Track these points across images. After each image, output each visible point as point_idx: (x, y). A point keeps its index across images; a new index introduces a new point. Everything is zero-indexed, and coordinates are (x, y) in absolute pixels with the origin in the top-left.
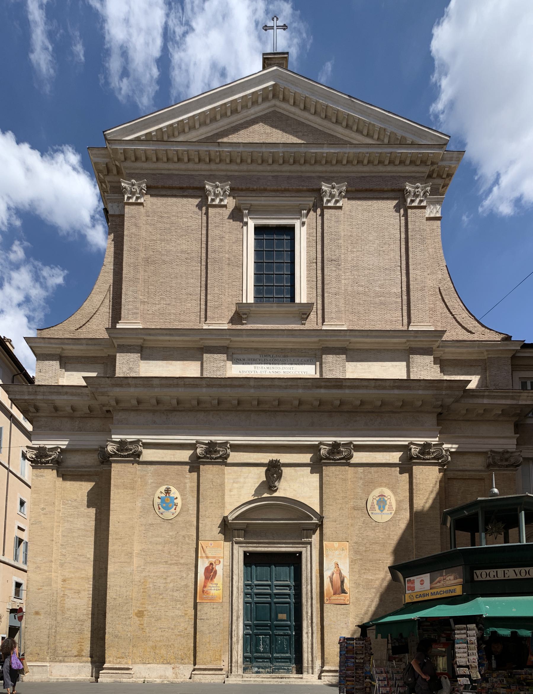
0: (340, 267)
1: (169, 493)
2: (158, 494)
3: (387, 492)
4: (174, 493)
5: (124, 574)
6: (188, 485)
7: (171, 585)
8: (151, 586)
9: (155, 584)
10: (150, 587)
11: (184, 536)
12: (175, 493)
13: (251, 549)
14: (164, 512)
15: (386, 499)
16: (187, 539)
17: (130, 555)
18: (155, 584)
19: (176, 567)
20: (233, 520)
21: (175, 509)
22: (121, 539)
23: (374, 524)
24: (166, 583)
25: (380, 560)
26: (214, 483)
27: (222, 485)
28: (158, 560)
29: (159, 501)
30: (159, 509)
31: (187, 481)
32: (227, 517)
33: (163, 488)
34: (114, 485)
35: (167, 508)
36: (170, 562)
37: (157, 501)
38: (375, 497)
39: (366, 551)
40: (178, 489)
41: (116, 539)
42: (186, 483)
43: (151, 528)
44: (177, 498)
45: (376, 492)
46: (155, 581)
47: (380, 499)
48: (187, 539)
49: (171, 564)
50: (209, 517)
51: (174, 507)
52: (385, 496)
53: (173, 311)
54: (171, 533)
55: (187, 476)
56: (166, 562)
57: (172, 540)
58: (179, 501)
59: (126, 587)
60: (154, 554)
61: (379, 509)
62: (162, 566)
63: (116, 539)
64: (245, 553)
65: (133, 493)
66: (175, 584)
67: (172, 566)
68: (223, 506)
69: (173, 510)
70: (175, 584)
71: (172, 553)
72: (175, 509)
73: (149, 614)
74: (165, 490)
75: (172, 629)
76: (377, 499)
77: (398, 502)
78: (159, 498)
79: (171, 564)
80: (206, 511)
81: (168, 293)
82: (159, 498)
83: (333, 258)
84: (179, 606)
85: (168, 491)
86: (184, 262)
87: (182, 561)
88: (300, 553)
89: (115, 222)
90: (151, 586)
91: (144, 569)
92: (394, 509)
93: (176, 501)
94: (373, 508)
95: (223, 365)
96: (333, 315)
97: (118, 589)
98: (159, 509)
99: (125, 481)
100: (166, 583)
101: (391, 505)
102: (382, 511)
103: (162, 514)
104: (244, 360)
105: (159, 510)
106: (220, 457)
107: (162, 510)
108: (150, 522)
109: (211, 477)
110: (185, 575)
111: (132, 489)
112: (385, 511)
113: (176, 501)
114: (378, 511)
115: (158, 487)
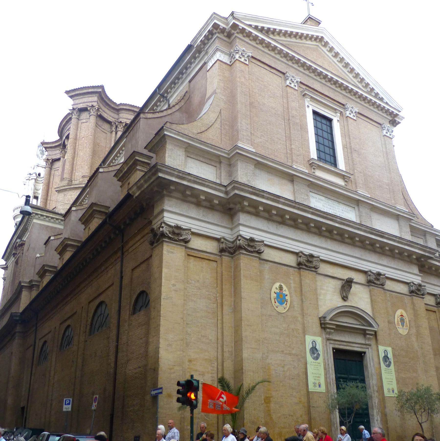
0: (360, 156)
1: (282, 290)
2: (274, 290)
3: (404, 314)
4: (285, 290)
6: (292, 285)
7: (288, 374)
8: (274, 373)
11: (293, 329)
12: (286, 291)
13: (337, 346)
14: (278, 306)
16: (295, 332)
18: (276, 371)
20: (330, 320)
21: (286, 305)
23: (400, 335)
24: (284, 371)
25: (406, 363)
27: (316, 290)
29: (275, 295)
30: (275, 302)
31: (292, 282)
32: (325, 318)
33: (277, 285)
35: (281, 303)
36: (285, 352)
37: (273, 295)
38: (398, 316)
39: (398, 355)
40: (287, 287)
41: (248, 325)
42: (291, 283)
43: (270, 319)
44: (287, 295)
45: (399, 312)
46: (276, 369)
48: (295, 332)
49: (286, 354)
50: (310, 316)
51: (286, 302)
53: (270, 147)
54: (284, 326)
55: (291, 277)
56: (283, 351)
57: (286, 332)
58: (288, 298)
59: (257, 373)
60: (273, 343)
61: (402, 325)
63: (248, 325)
64: (333, 349)
65: (257, 286)
67: (287, 356)
68: (317, 307)
69: (284, 305)
71: (286, 344)
72: (286, 305)
73: (274, 400)
74: (279, 287)
75: (292, 416)
76: (400, 317)
77: (409, 321)
78: (275, 292)
79: (286, 354)
81: (265, 133)
82: (275, 292)
83: (356, 149)
84: (294, 394)
85: (281, 288)
87: (294, 352)
88: (365, 353)
90: (274, 373)
91: (267, 356)
92: (408, 326)
93: (287, 298)
94: (398, 324)
95: (307, 199)
96: (361, 185)
97: (252, 374)
98: (275, 302)
99: (251, 273)
101: (406, 323)
103: (277, 307)
104: (316, 198)
105: (275, 304)
107: (277, 304)
109: (308, 281)
110: (296, 365)
112: (404, 327)
113: (287, 298)
114: (401, 326)
115: (274, 283)
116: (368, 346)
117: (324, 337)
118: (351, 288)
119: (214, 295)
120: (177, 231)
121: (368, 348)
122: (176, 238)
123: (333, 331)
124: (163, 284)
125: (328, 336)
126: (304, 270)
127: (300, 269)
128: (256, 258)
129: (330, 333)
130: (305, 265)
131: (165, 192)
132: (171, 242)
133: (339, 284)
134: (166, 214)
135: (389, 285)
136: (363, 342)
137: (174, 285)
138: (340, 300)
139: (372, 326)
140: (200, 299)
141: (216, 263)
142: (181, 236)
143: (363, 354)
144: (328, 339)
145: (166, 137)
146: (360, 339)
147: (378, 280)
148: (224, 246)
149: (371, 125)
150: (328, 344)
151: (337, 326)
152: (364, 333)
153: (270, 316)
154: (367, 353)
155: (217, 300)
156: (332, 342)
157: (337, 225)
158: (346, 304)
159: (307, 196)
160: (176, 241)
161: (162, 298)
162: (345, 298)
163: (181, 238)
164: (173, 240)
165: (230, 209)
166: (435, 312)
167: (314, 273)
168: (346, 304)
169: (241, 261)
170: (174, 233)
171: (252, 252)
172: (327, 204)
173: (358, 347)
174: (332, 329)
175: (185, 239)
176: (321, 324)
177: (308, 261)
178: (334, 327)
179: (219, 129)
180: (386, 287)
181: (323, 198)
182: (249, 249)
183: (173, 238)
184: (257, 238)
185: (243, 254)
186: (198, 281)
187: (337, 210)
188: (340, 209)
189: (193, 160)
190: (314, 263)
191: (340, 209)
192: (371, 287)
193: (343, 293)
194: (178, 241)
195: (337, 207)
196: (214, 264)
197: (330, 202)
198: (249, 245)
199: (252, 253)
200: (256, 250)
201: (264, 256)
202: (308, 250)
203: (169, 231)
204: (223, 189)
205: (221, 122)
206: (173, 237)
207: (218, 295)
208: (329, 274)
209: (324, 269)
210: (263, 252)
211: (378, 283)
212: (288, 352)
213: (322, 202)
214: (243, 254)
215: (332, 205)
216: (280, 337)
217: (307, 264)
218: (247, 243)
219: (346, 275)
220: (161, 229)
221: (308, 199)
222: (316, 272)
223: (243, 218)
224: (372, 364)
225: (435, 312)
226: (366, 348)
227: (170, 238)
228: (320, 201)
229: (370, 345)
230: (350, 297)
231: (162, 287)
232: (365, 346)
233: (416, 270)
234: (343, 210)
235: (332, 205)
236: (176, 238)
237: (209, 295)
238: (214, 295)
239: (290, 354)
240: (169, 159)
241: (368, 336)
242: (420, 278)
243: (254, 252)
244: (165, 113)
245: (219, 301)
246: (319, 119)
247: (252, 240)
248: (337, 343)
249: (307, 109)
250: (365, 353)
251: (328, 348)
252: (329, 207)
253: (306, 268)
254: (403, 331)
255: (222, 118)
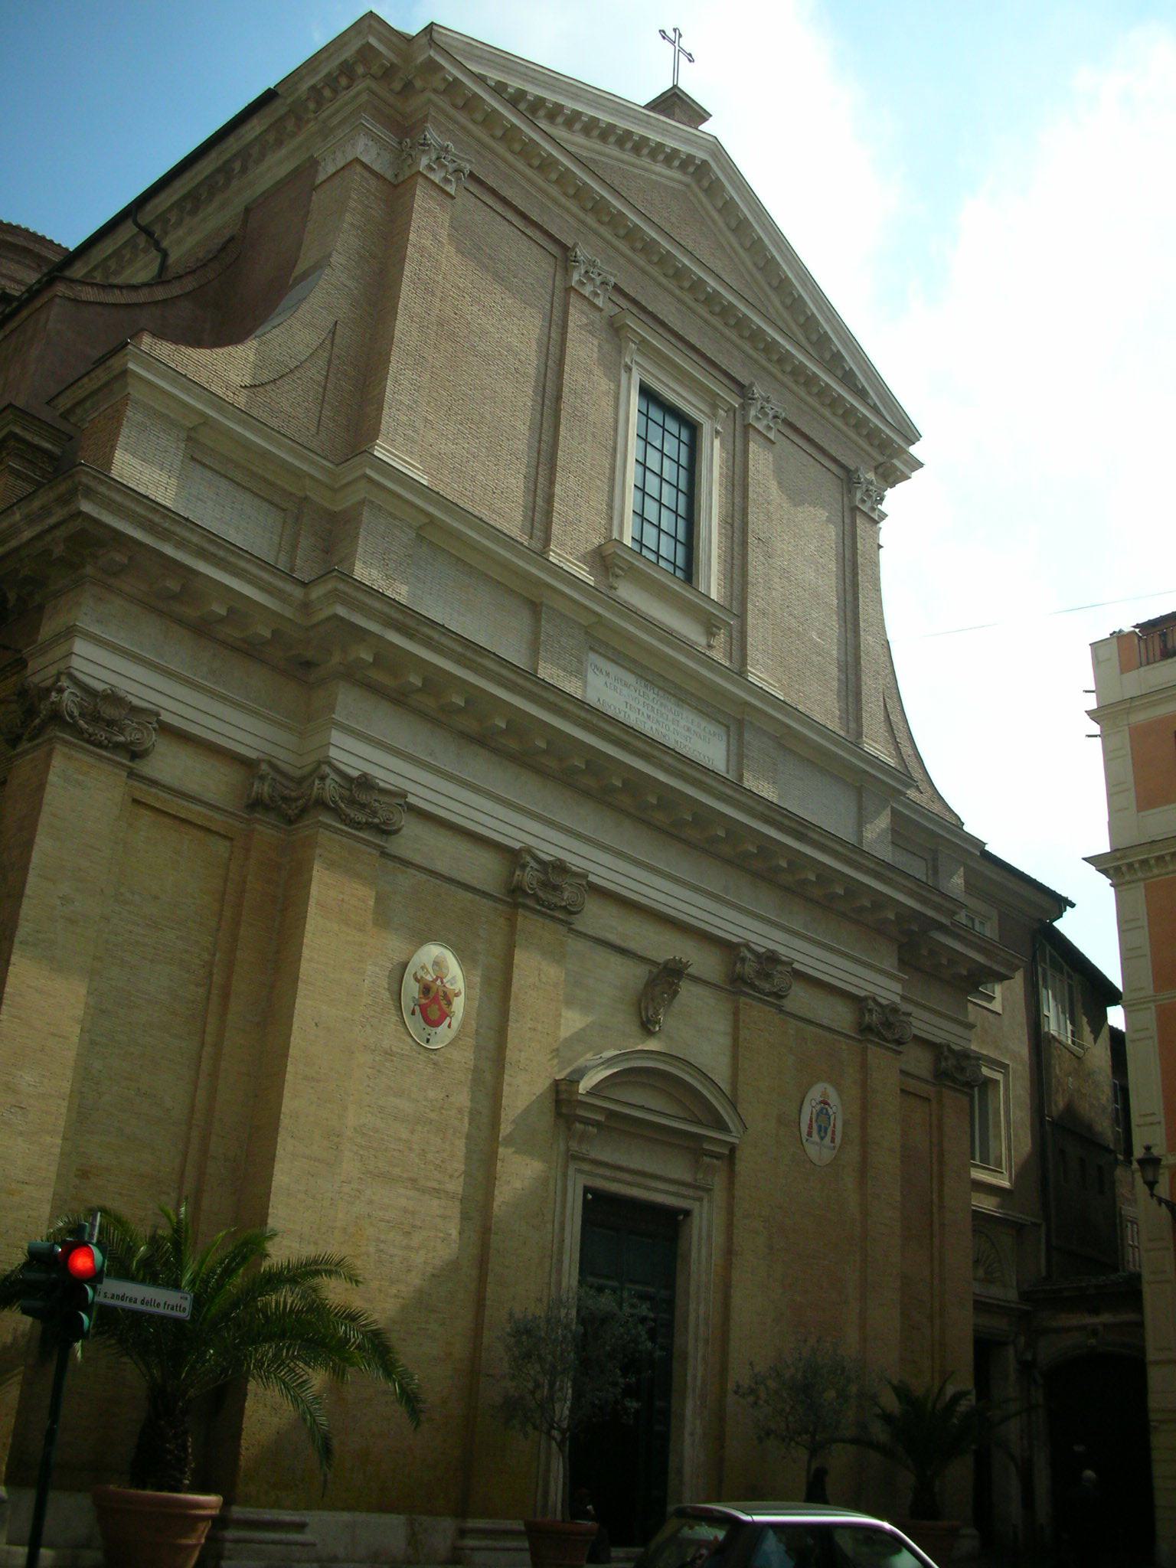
3: (833, 1098)
5: (314, 1197)
8: (372, 1249)
9: (382, 1246)
10: (368, 1255)
15: (830, 1111)
17: (336, 1140)
18: (382, 1246)
19: (435, 1202)
21: (449, 1026)
22: (318, 1081)
26: (542, 975)
28: (397, 1171)
34: (318, 903)
45: (816, 1093)
46: (383, 1237)
47: (822, 1109)
52: (828, 1104)
54: (431, 1094)
56: (414, 1180)
57: (433, 1116)
60: (386, 1150)
62: (402, 1191)
64: (587, 1190)
66: (430, 1255)
67: (427, 1197)
70: (430, 1255)
71: (430, 1156)
77: (845, 1123)
80: (520, 1051)
83: (762, 536)
86: (512, 374)
88: (687, 1213)
89: (369, 184)
100: (408, 1248)
102: (822, 1138)
104: (608, 674)
106: (564, 908)
108: (386, 1044)
111: (360, 930)
114: (815, 1137)
116: (701, 1193)
117: (562, 1148)
118: (676, 993)
119: (206, 956)
120: (109, 711)
121: (700, 1199)
122: (102, 735)
123: (594, 1130)
124: (28, 891)
125: (574, 1145)
126: (528, 914)
127: (516, 906)
128: (369, 850)
129: (583, 1138)
130: (538, 900)
131: (89, 570)
132: (82, 748)
133: (634, 975)
134: (80, 646)
135: (800, 999)
136: (688, 1178)
137: (65, 900)
138: (634, 1029)
139: (724, 1128)
140: (152, 961)
141: (227, 843)
142: (121, 731)
143: (681, 1217)
144: (572, 1157)
145: (130, 380)
146: (677, 1168)
147: (768, 976)
148: (264, 789)
149: (819, 466)
150: (571, 1172)
151: (611, 1114)
152: (693, 1147)
153: (389, 1053)
154: (696, 1213)
155: (211, 974)
156: (586, 1167)
157: (662, 777)
158: (652, 1045)
159: (580, 661)
160: (100, 745)
161: (16, 940)
162: (647, 1027)
163: (121, 739)
164: (88, 741)
165: (308, 665)
166: (928, 1100)
167: (563, 929)
168: (652, 1045)
169: (318, 851)
170: (95, 718)
171: (358, 826)
172: (642, 699)
173: (667, 1192)
174: (597, 1124)
175: (132, 743)
176: (558, 1102)
177: (545, 885)
178: (600, 1118)
179: (319, 385)
180: (789, 1004)
181: (631, 679)
182: (352, 816)
183: (90, 735)
184: (384, 778)
185: (328, 827)
186: (156, 898)
187: (670, 723)
188: (683, 723)
189: (208, 474)
190: (566, 895)
191: (683, 723)
192: (743, 999)
193: (647, 1009)
194: (105, 748)
195: (671, 716)
196: (221, 847)
197: (652, 696)
198: (352, 802)
199: (359, 829)
200: (376, 820)
201: (400, 846)
202: (551, 845)
203: (80, 706)
204: (298, 592)
205: (330, 362)
206: (91, 730)
207: (218, 956)
208: (612, 937)
209: (598, 918)
210: (396, 832)
211: (767, 986)
212: (435, 1185)
213: (625, 691)
214: (328, 827)
215: (656, 707)
216: (412, 1132)
217: (541, 894)
218: (347, 793)
219: (664, 946)
220: (54, 694)
221: (579, 673)
222: (567, 923)
223: (348, 703)
224: (704, 1251)
225: (928, 1100)
226: (695, 1199)
227: (79, 733)
228: (619, 686)
229: (708, 1190)
230: (667, 1021)
231: (25, 901)
232: (691, 1192)
233: (890, 963)
234: (689, 730)
235: (656, 707)
236: (102, 735)
237: (187, 951)
238: (206, 956)
239: (436, 1192)
240: (128, 457)
241: (707, 1159)
242: (897, 987)
243: (369, 826)
244: (142, 296)
245: (218, 978)
246: (656, 414)
247: (365, 783)
248: (601, 1171)
249: (624, 377)
250: (687, 1213)
251: (570, 1184)
252: (644, 710)
253: (539, 908)
254: (818, 1151)
255: (336, 349)
